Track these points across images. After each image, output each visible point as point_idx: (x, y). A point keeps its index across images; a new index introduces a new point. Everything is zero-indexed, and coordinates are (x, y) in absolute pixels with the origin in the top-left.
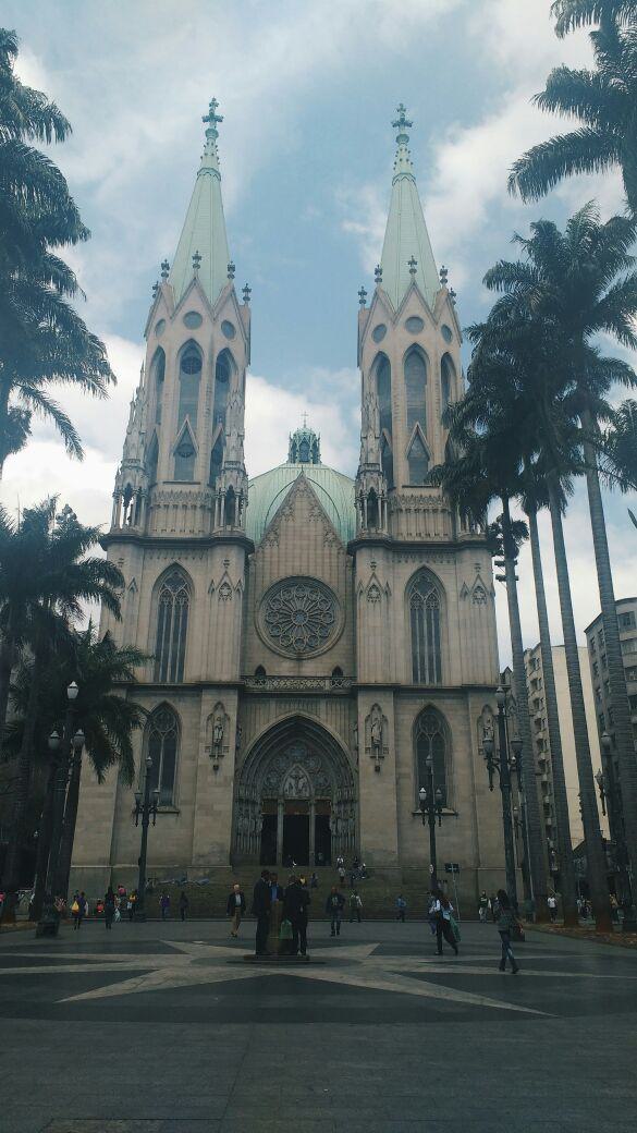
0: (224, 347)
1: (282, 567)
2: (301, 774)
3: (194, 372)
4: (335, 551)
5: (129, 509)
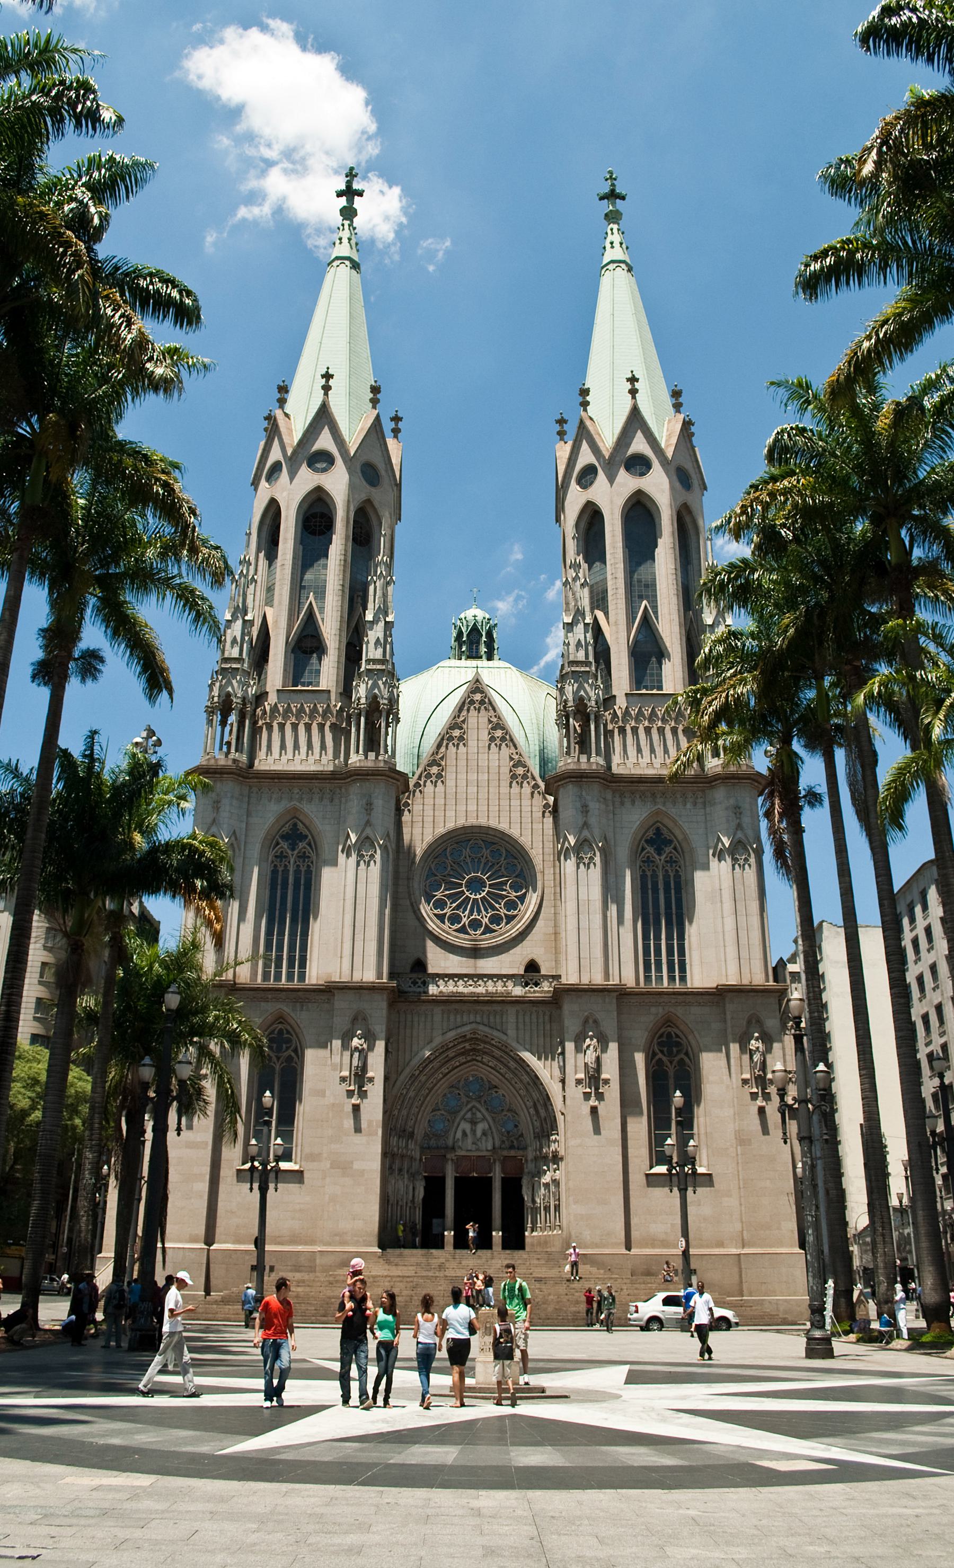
0: (363, 497)
1: (451, 814)
2: (479, 1115)
3: (322, 533)
4: (527, 789)
5: (227, 729)
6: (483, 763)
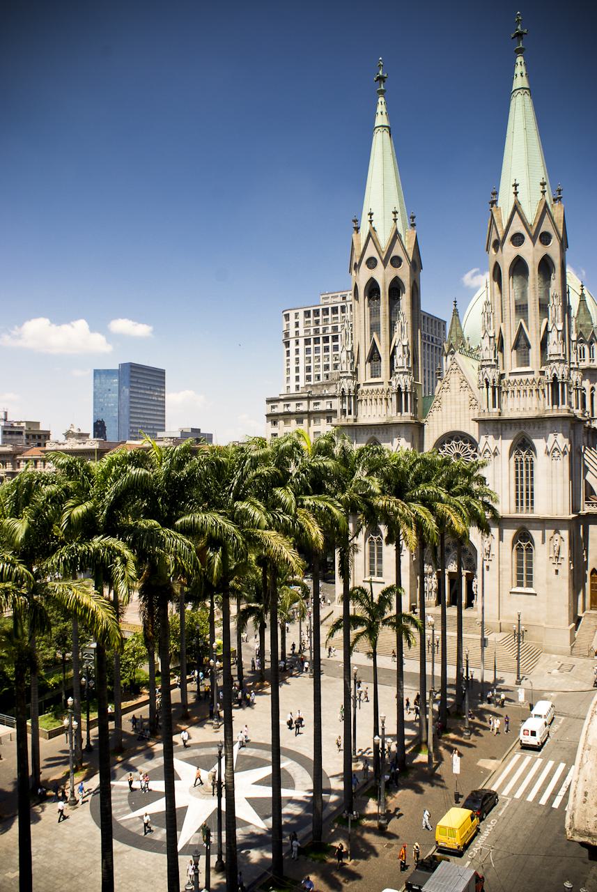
0: (393, 277)
6: (458, 400)
